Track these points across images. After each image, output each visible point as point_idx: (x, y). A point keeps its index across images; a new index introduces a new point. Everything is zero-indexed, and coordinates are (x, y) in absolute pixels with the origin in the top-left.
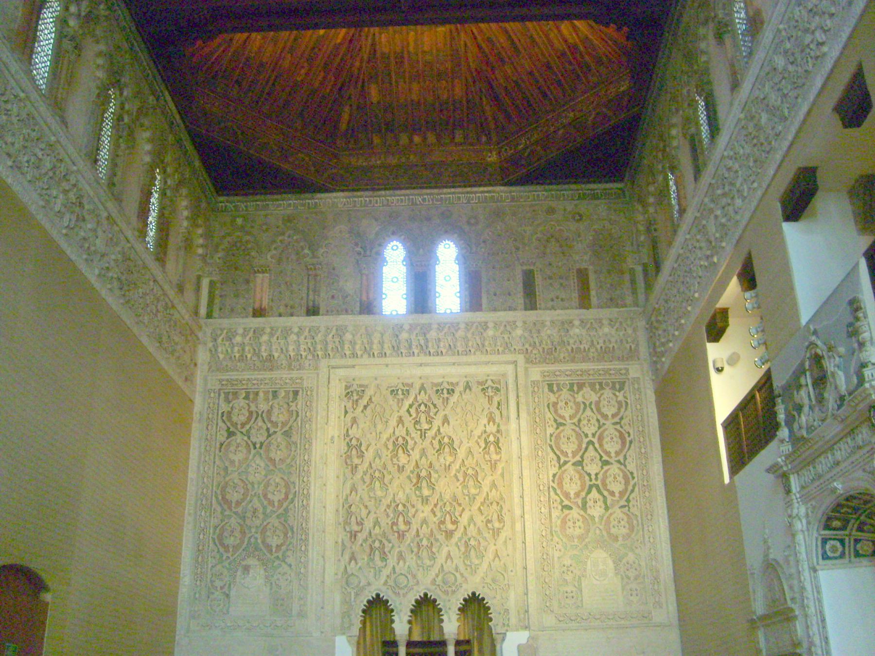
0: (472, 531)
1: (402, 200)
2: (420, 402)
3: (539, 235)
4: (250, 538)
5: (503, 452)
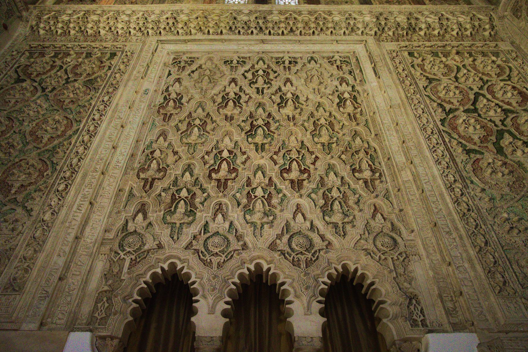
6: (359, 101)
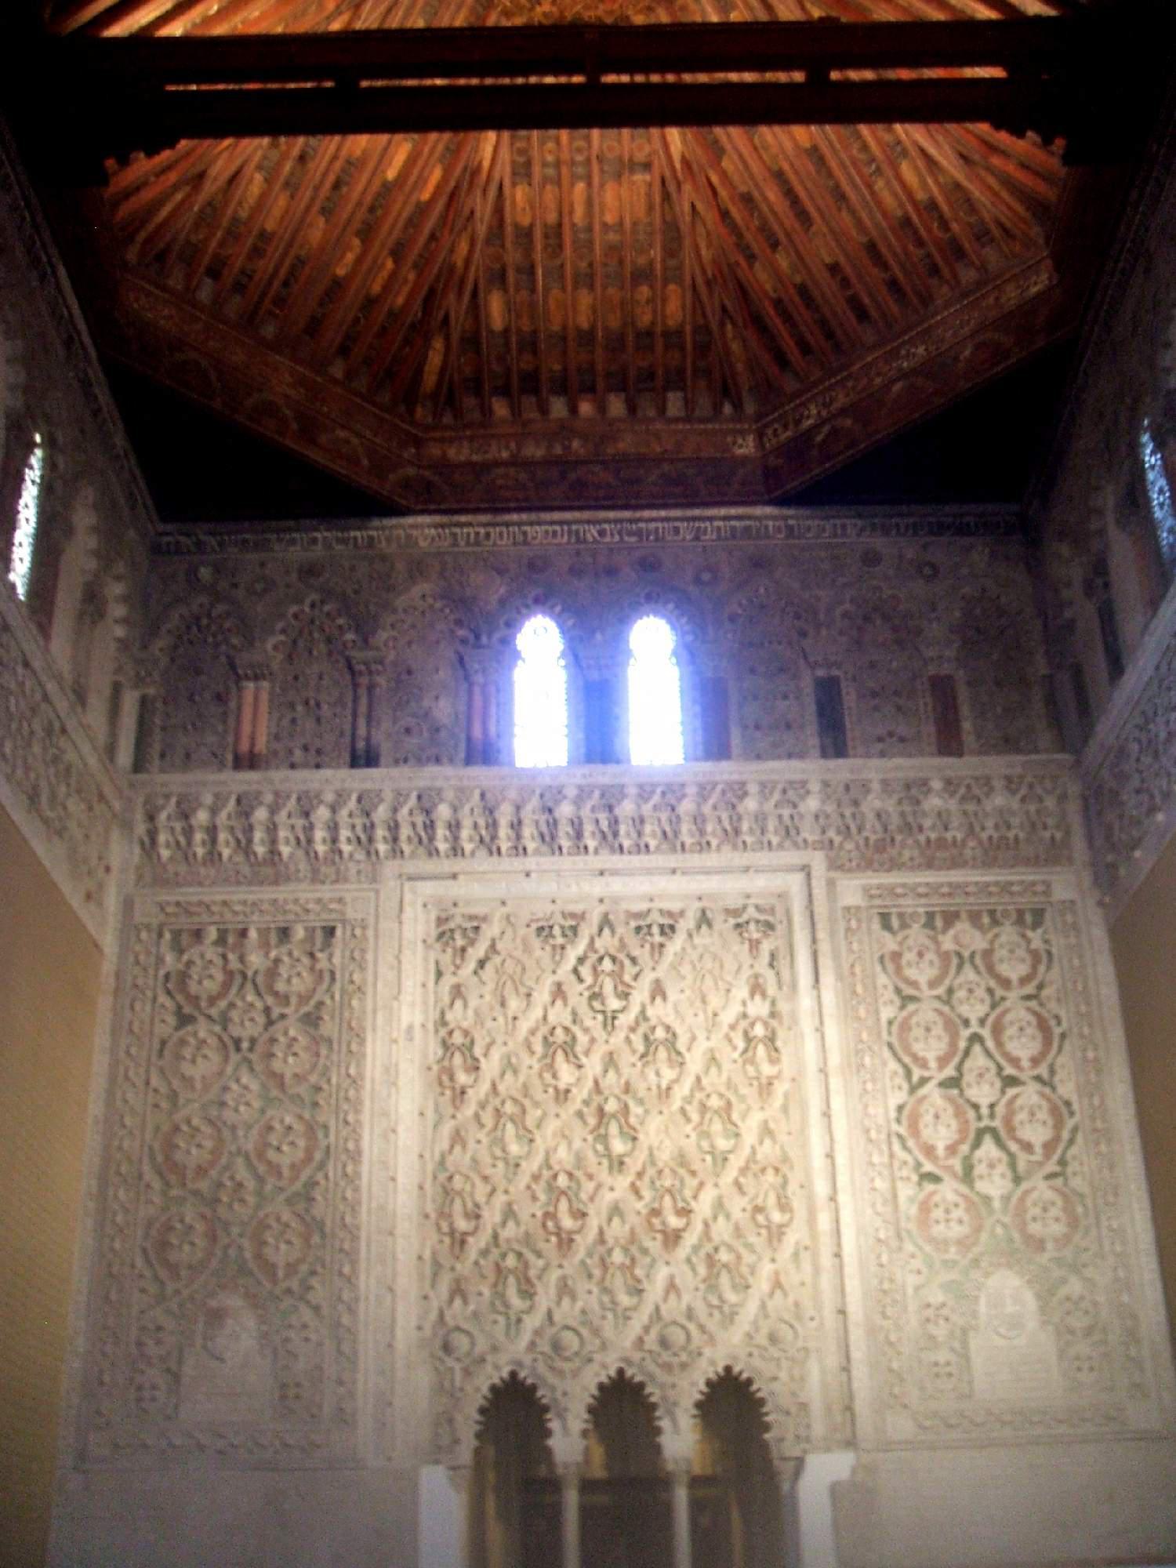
0: (722, 1230)
1: (555, 533)
2: (602, 952)
3: (848, 606)
4: (228, 1246)
5: (785, 1058)
6: (779, 1044)
